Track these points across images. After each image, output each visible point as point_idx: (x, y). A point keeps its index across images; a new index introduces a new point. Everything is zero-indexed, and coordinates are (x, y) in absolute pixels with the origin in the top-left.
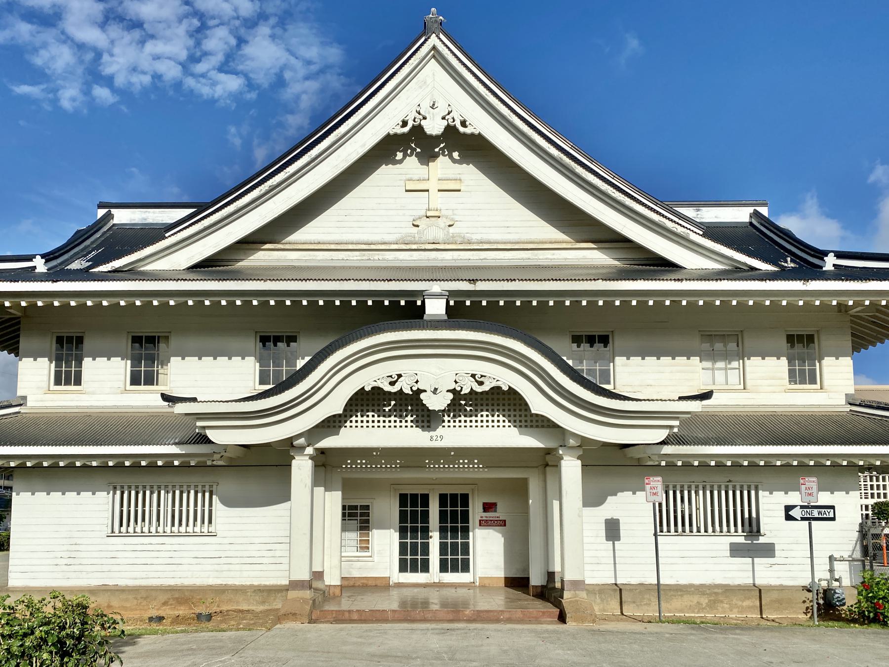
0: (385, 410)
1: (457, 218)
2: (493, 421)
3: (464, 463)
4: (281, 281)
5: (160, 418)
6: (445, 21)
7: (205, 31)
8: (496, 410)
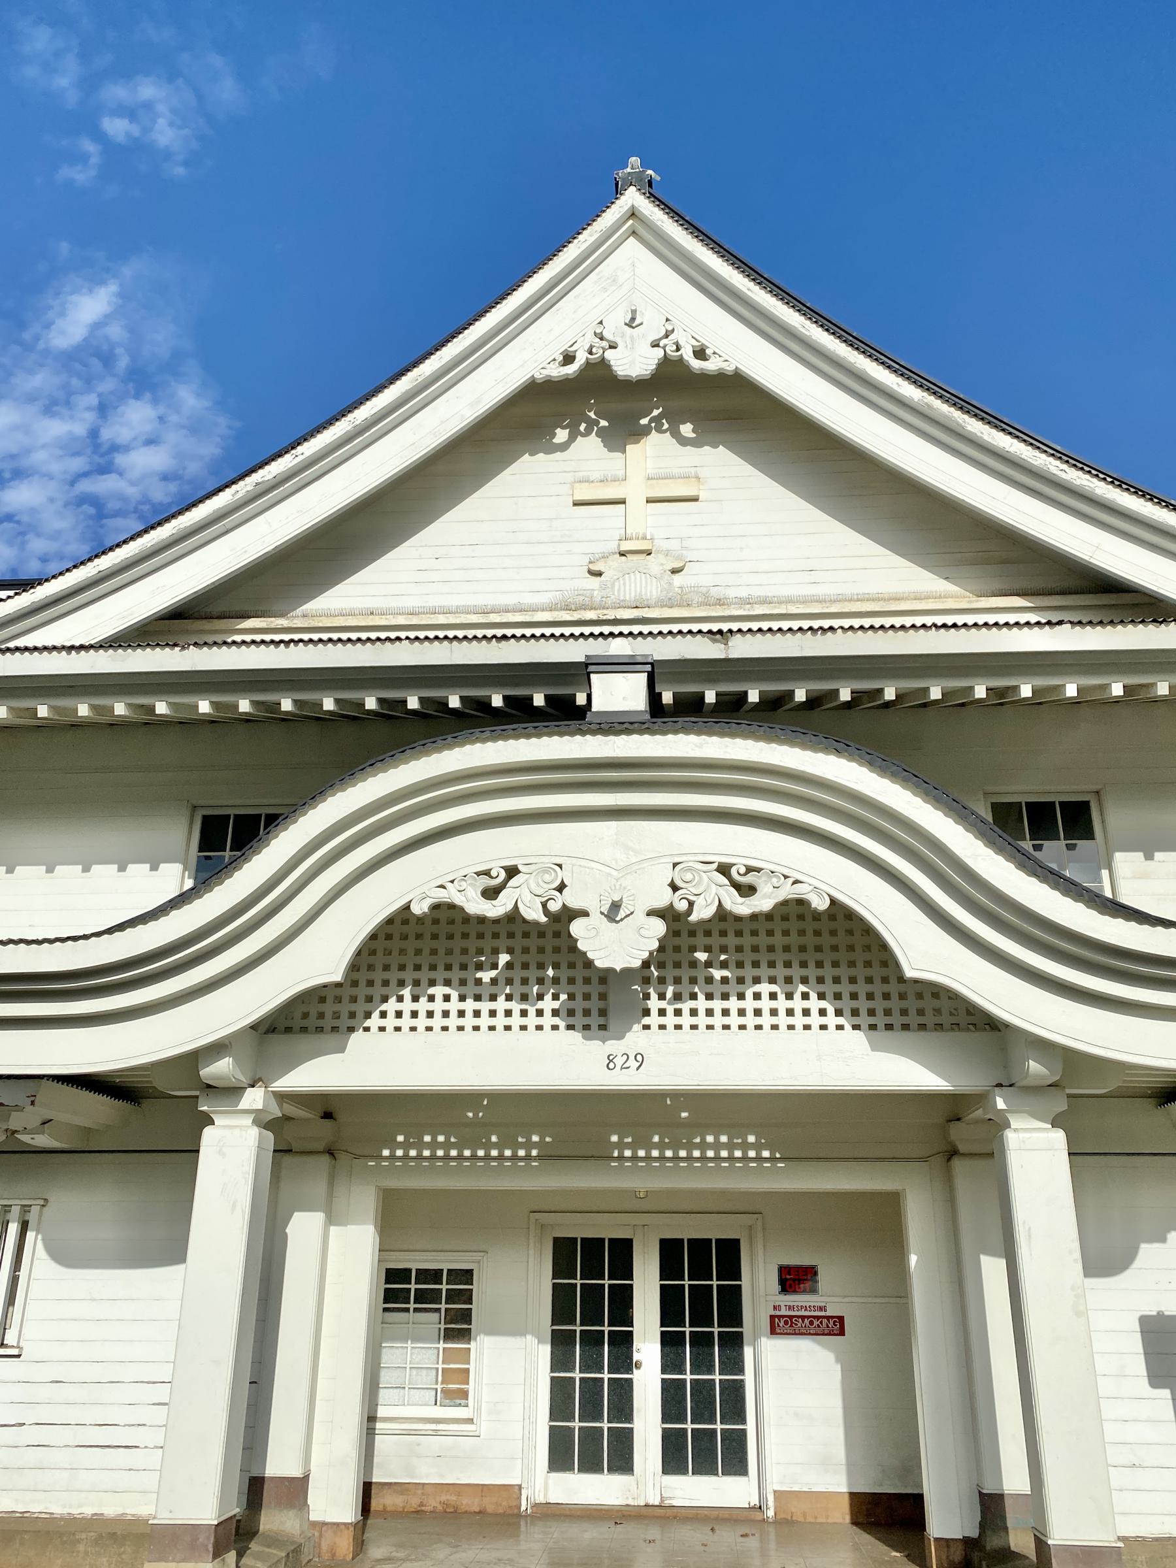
6: (658, 178)
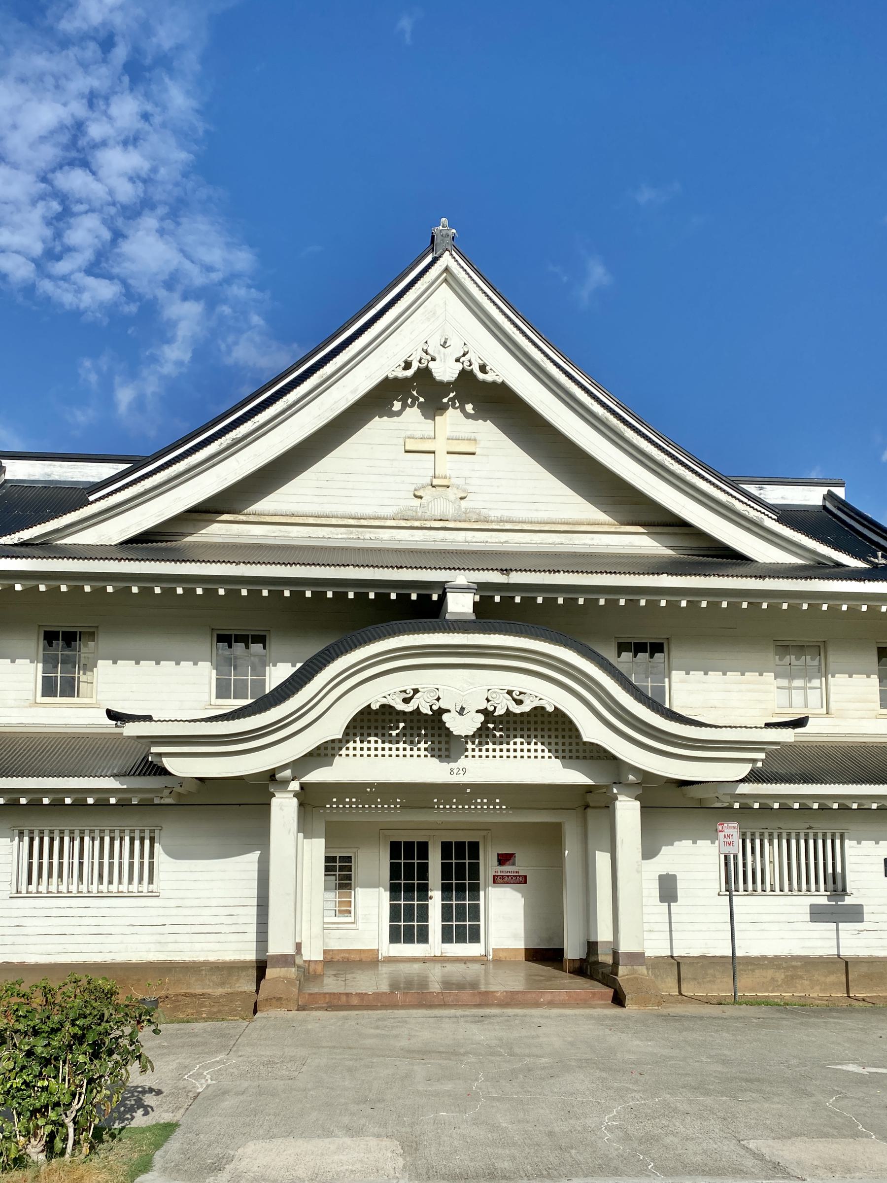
0: (391, 734)
1: (470, 489)
2: (529, 751)
3: (482, 804)
4: (273, 565)
5: (85, 740)
8: (532, 736)
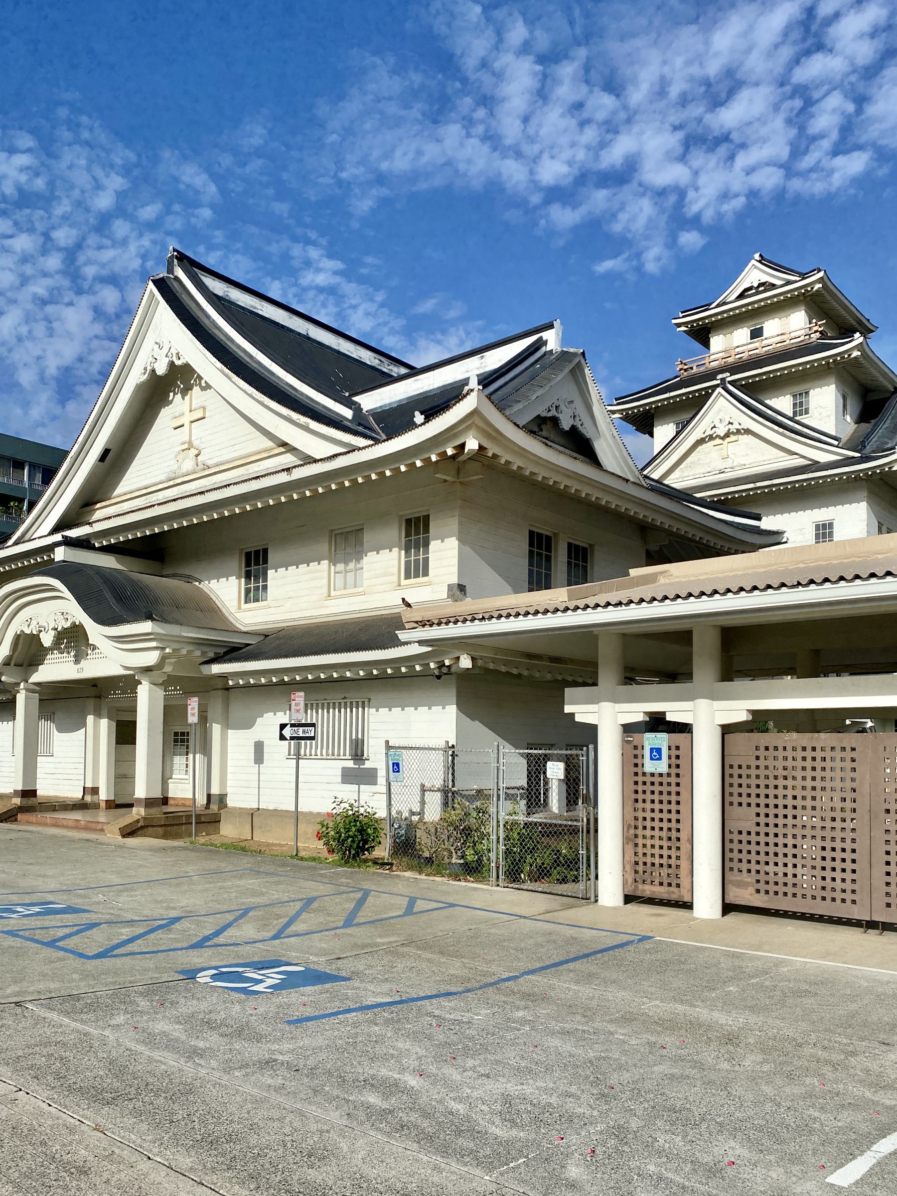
7: (810, 109)
